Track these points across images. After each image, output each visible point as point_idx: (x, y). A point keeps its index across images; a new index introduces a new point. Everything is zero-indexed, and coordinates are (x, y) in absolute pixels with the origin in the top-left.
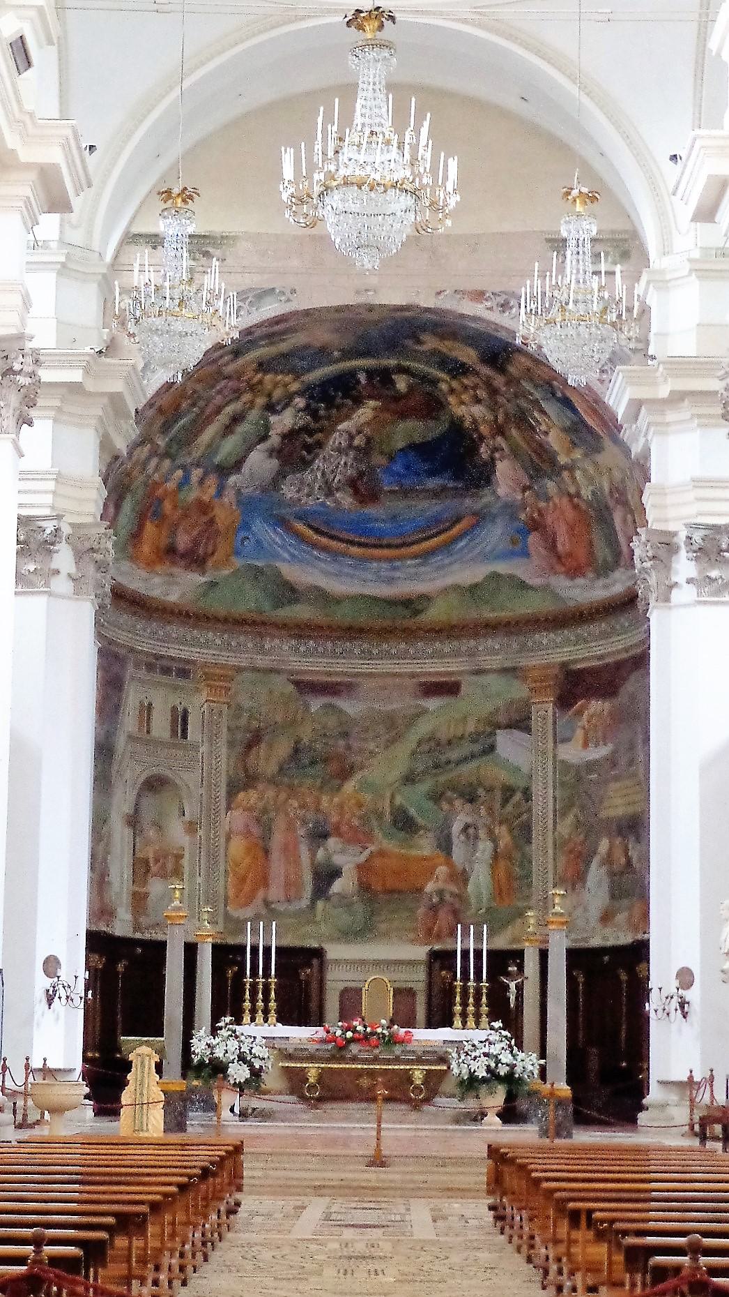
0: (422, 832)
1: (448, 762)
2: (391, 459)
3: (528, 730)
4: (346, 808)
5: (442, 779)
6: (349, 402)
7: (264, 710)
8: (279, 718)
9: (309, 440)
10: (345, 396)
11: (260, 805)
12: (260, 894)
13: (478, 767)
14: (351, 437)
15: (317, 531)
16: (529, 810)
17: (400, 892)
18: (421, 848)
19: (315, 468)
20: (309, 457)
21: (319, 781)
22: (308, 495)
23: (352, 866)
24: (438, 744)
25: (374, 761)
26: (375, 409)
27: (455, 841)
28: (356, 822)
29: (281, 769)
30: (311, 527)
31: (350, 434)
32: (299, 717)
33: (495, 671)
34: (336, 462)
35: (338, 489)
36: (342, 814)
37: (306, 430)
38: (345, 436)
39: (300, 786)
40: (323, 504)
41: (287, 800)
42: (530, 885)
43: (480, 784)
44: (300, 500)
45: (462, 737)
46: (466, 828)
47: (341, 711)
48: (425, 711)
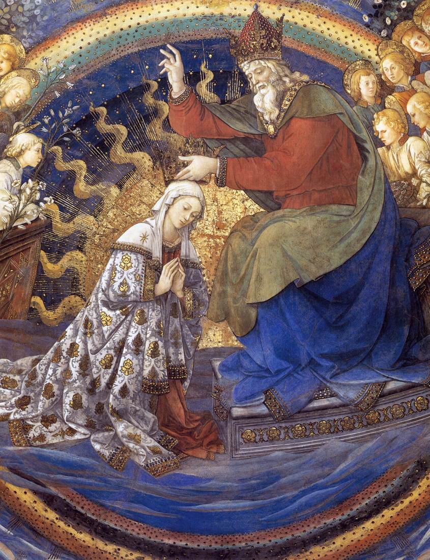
2: (249, 333)
6: (143, 159)
9: (53, 269)
10: (137, 142)
14: (154, 270)
15: (67, 512)
19: (65, 347)
20: (50, 316)
22: (47, 420)
26: (201, 182)
30: (50, 500)
31: (147, 255)
34: (118, 337)
35: (120, 414)
37: (42, 227)
38: (136, 263)
40: (85, 445)
44: (26, 428)
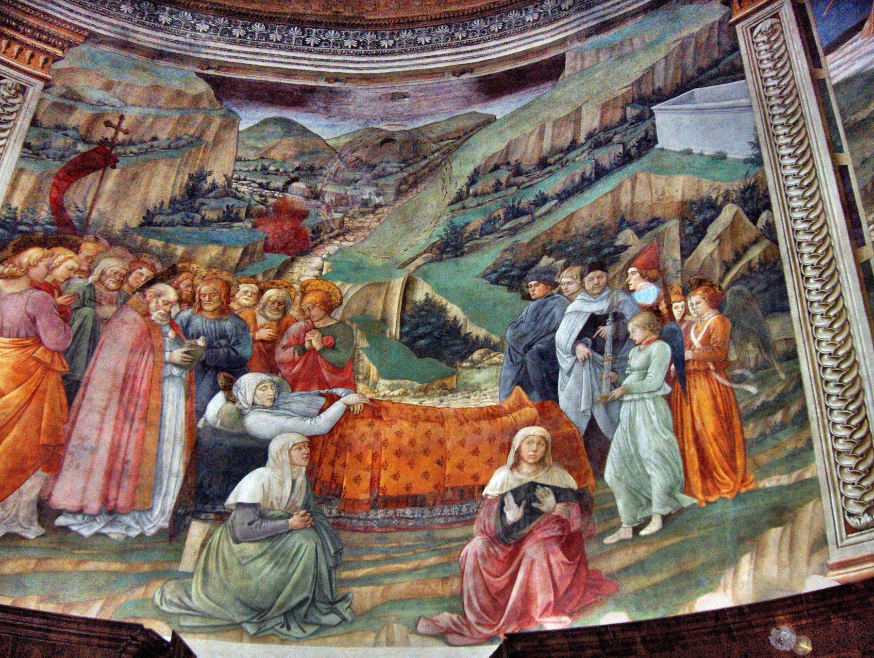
0: (476, 355)
1: (543, 200)
3: (735, 73)
4: (294, 312)
5: (525, 237)
7: (132, 114)
8: (164, 134)
11: (79, 283)
12: (32, 487)
13: (616, 192)
16: (770, 230)
17: (415, 501)
18: (476, 388)
21: (237, 254)
23: (296, 438)
24: (518, 171)
25: (370, 220)
27: (564, 362)
28: (314, 341)
29: (148, 221)
32: (210, 136)
33: (634, 14)
36: (282, 327)
39: (188, 258)
41: (150, 283)
42: (802, 419)
43: (622, 223)
45: (573, 145)
46: (595, 321)
47: (304, 131)
48: (490, 120)
